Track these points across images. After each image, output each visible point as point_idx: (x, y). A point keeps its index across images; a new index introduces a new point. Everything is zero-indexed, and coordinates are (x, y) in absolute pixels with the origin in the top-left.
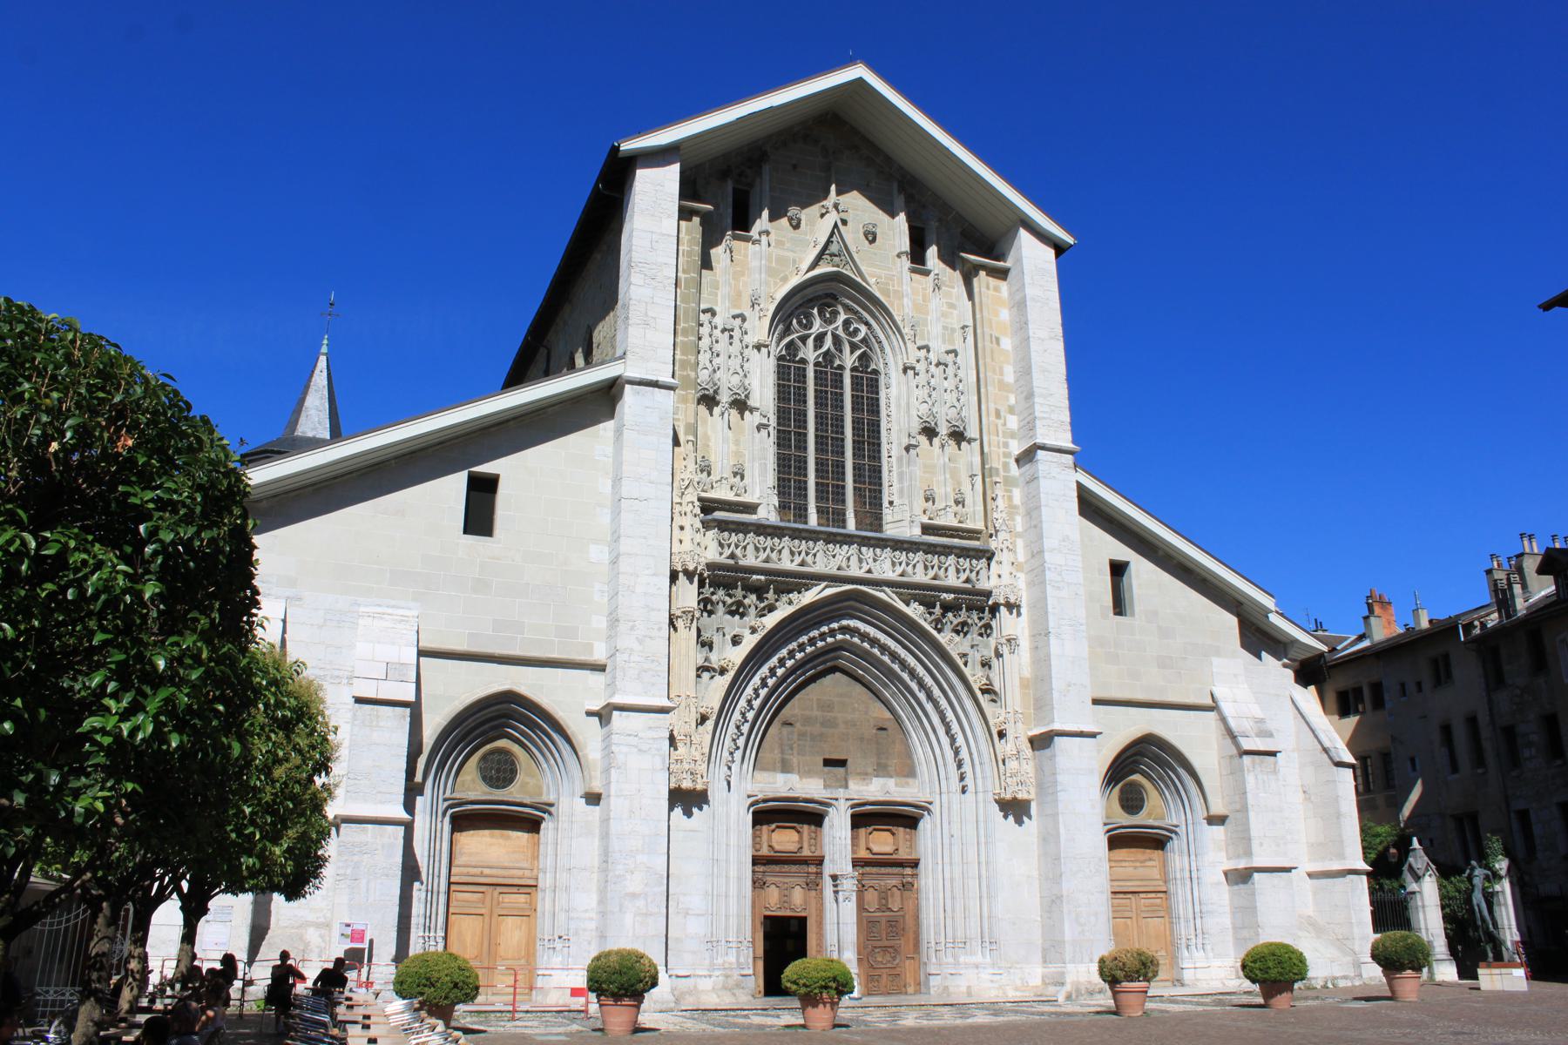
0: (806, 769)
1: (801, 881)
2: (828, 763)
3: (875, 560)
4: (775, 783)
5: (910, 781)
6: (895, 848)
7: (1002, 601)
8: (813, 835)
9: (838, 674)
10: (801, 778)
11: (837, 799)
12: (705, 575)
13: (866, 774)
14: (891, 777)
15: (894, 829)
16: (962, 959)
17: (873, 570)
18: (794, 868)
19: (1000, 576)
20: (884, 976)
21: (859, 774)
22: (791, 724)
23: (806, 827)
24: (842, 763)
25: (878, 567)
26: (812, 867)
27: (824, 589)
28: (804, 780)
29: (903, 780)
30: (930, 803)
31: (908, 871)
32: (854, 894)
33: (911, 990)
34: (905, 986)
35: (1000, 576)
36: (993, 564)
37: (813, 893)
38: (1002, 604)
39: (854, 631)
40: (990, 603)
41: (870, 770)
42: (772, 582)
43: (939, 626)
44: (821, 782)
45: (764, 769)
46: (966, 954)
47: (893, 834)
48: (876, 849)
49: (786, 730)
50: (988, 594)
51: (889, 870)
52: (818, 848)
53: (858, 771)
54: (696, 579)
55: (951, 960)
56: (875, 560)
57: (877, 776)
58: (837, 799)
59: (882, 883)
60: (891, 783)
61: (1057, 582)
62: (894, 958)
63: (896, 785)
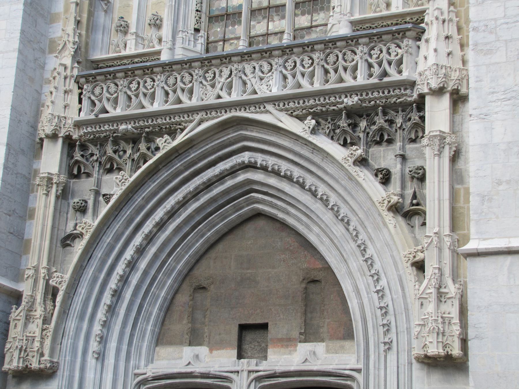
2: (243, 328)
3: (261, 79)
4: (181, 358)
5: (347, 344)
7: (426, 90)
9: (261, 223)
10: (211, 350)
12: (75, 136)
14: (322, 341)
17: (258, 91)
19: (426, 58)
21: (281, 340)
22: (204, 288)
24: (264, 327)
25: (264, 86)
27: (199, 124)
28: (215, 352)
29: (339, 343)
30: (358, 371)
35: (426, 58)
36: (422, 43)
38: (428, 94)
39: (251, 166)
40: (415, 96)
41: (295, 334)
42: (142, 128)
43: (349, 141)
44: (235, 352)
45: (170, 343)
49: (199, 296)
50: (412, 84)
54: (60, 141)
56: (261, 79)
57: (305, 341)
58: (238, 372)
60: (320, 348)
61: (486, 44)
63: (328, 351)
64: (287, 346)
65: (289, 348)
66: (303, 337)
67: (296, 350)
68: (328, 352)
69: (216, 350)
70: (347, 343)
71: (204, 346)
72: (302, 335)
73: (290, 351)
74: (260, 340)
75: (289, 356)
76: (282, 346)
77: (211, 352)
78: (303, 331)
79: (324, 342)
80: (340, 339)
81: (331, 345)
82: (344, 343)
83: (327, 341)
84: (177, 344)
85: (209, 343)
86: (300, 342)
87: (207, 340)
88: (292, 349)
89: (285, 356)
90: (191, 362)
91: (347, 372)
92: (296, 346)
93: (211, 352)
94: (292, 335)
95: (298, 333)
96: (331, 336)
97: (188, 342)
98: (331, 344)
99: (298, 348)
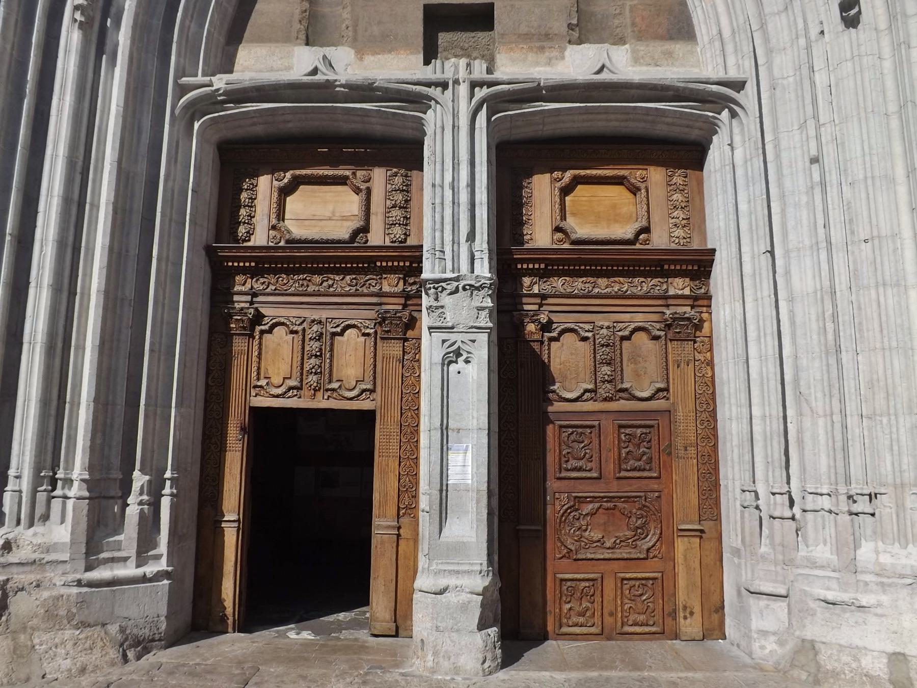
0: (376, 30)
1: (365, 316)
4: (289, 68)
5: (679, 48)
6: (637, 226)
8: (399, 197)
10: (360, 54)
11: (444, 85)
13: (547, 36)
15: (635, 174)
16: (866, 552)
18: (344, 283)
20: (609, 585)
21: (526, 37)
23: (379, 175)
26: (393, 278)
28: (369, 59)
29: (657, 48)
31: (679, 286)
32: (483, 338)
33: (691, 626)
34: (674, 614)
37: (395, 349)
41: (559, 26)
46: (879, 534)
47: (634, 190)
48: (582, 229)
51: (621, 285)
52: (412, 227)
53: (523, 29)
55: (823, 552)
57: (580, 42)
58: (444, 85)
59: (602, 321)
62: (640, 532)
64: (542, 49)
65: (547, 54)
66: (576, 34)
67: (563, 58)
68: (636, 62)
69: (373, 55)
70: (678, 46)
71: (343, 45)
72: (572, 30)
73: (550, 59)
74: (466, 46)
75: (548, 69)
76: (531, 49)
77: (361, 59)
78: (575, 22)
79: (624, 43)
80: (662, 38)
81: (642, 48)
82: (673, 46)
83: (633, 41)
84: (277, 41)
85: (355, 39)
86: (570, 42)
87: (350, 34)
88: (555, 53)
89: (537, 69)
90: (320, 67)
91: (715, 88)
92: (563, 50)
93: (361, 59)
94: (550, 28)
95: (565, 25)
96: (640, 32)
97: (304, 37)
98: (642, 47)
99: (567, 53)
